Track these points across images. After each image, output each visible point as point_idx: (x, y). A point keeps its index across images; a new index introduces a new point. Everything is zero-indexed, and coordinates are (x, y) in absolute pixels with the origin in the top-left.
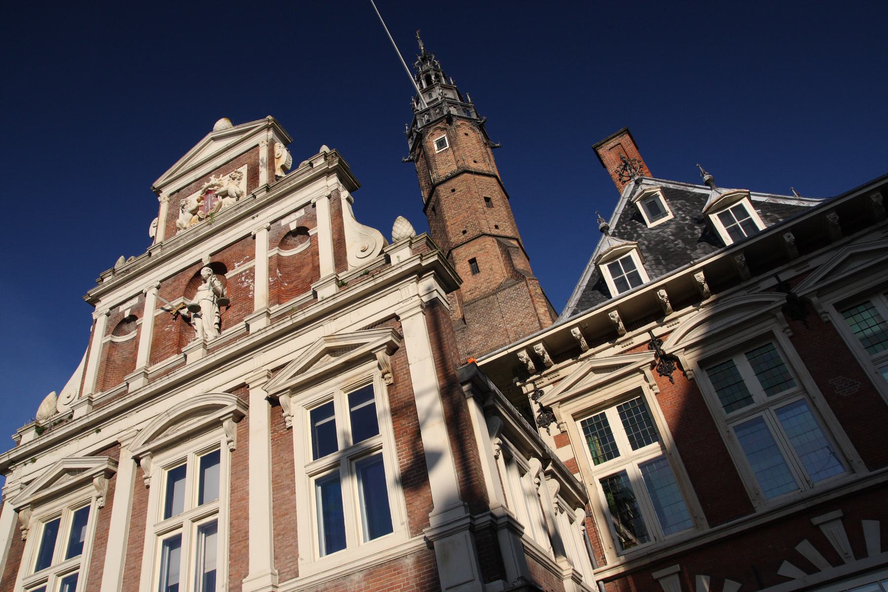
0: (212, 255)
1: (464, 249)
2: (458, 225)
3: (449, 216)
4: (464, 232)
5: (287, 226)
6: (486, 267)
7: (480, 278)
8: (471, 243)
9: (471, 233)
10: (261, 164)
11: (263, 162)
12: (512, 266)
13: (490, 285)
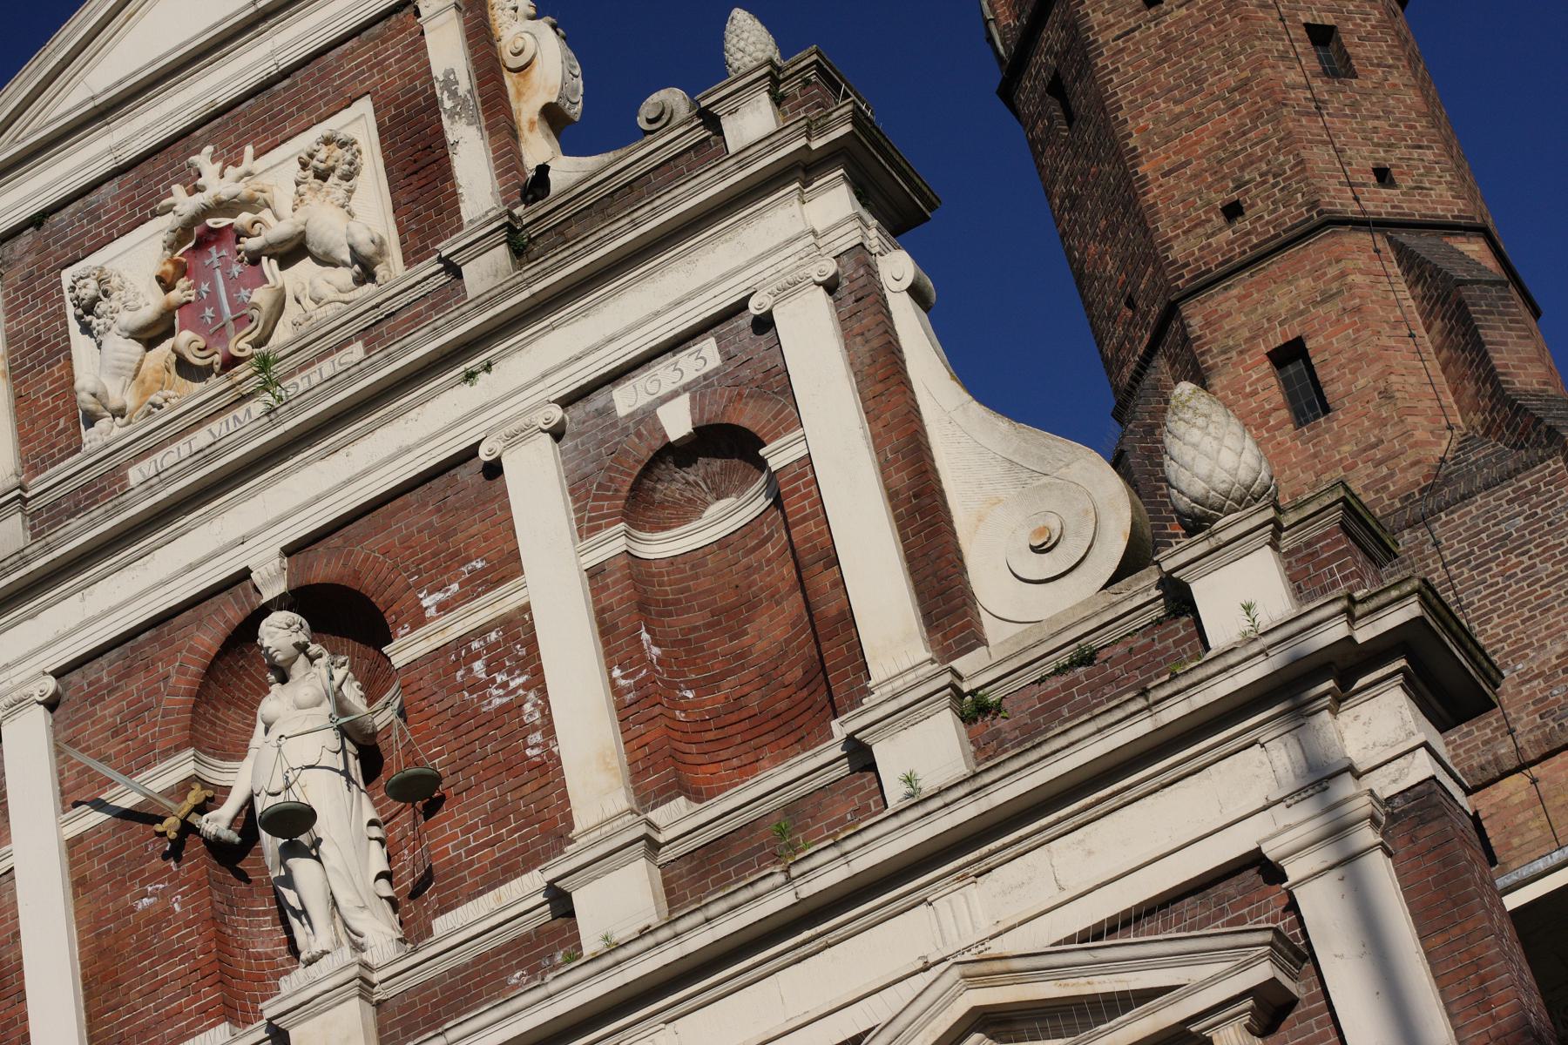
0: (290, 551)
1: (1240, 298)
2: (1194, 177)
3: (1145, 129)
4: (1233, 211)
5: (647, 417)
6: (1361, 382)
7: (1338, 441)
8: (1274, 266)
9: (1263, 217)
10: (448, 104)
11: (453, 94)
12: (1489, 377)
13: (1392, 475)
